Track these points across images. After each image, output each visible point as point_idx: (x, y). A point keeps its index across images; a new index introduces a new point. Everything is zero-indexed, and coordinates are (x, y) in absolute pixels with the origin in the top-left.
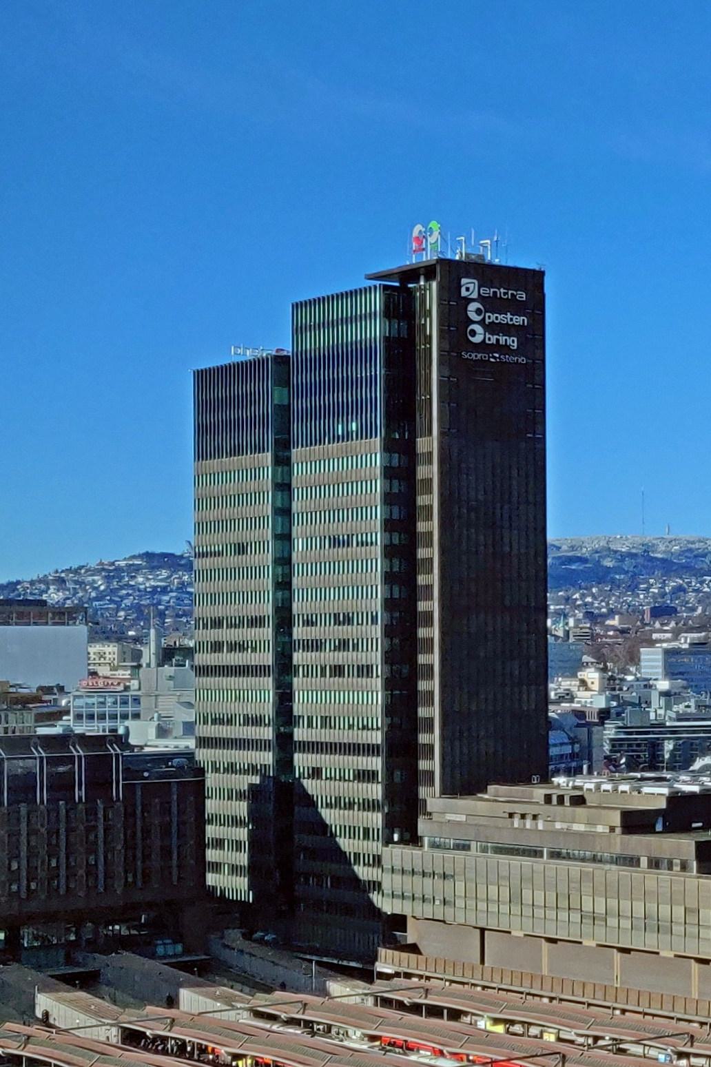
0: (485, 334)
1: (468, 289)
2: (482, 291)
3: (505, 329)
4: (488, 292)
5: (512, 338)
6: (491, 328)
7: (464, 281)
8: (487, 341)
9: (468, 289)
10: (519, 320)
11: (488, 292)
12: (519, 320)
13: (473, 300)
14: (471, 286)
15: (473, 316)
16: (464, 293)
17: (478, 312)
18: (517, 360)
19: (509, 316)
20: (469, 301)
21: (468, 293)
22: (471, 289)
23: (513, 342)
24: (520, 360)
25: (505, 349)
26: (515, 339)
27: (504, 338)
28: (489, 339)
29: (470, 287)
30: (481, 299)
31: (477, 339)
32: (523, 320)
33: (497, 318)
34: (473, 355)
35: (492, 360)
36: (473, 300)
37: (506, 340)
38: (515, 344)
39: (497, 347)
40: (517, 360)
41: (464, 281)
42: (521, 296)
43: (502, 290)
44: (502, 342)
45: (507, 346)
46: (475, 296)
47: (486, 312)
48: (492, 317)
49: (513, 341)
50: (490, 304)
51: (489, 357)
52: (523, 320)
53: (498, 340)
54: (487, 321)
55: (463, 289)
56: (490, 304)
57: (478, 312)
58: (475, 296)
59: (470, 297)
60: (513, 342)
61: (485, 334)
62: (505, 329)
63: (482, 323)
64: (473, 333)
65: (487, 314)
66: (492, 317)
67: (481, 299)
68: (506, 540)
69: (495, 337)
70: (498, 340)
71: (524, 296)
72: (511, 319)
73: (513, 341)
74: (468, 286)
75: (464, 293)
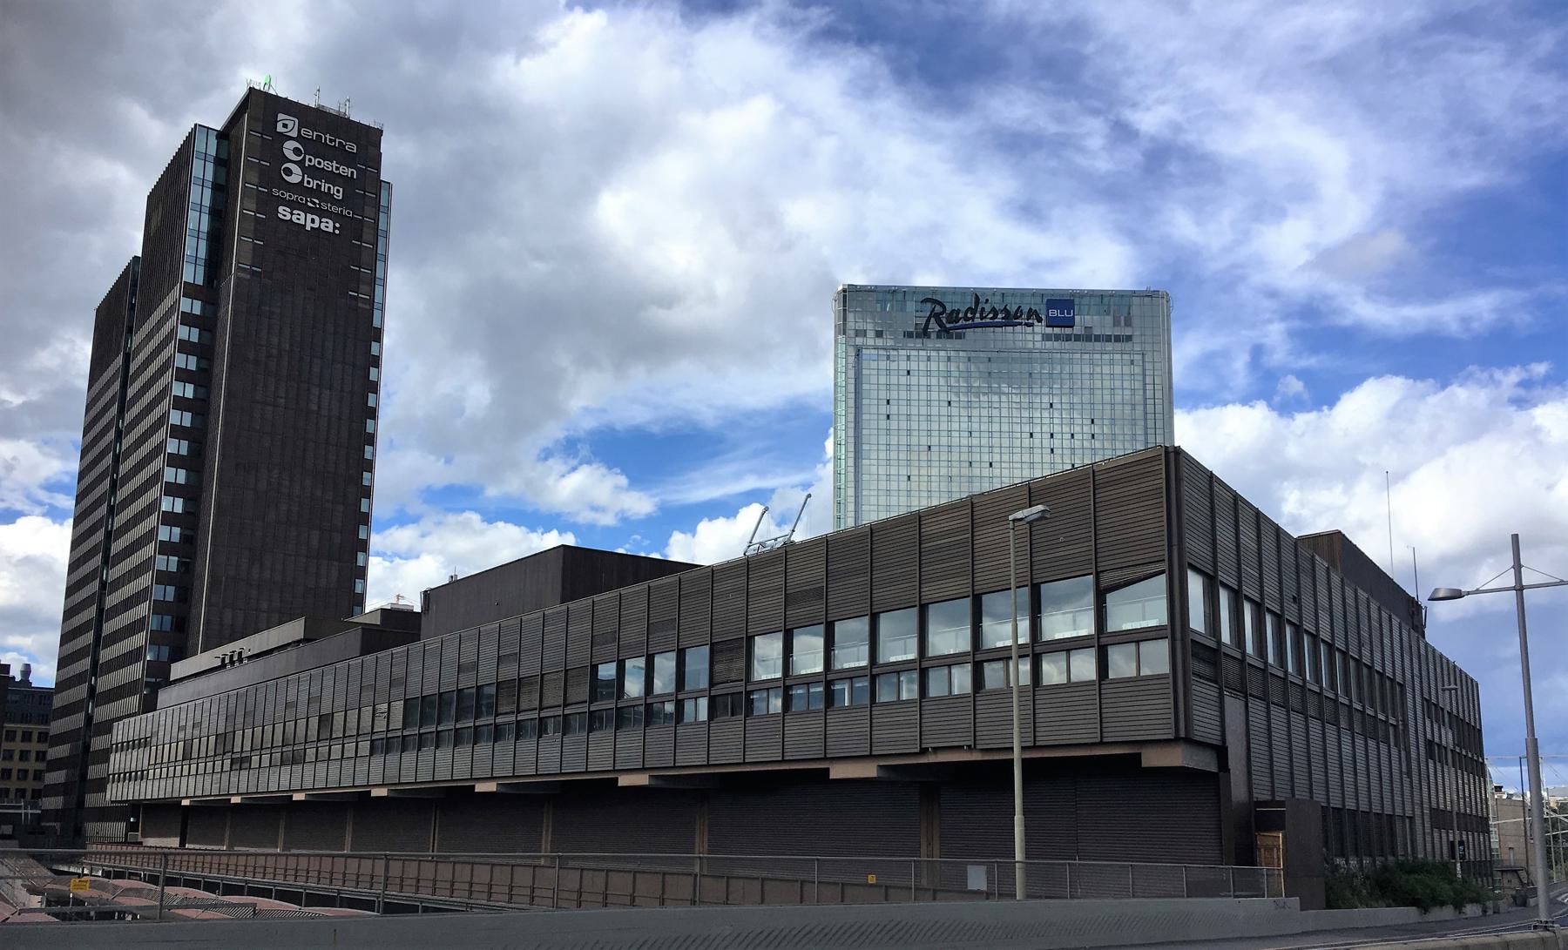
0: (303, 176)
1: (285, 126)
3: (333, 178)
7: (281, 116)
9: (285, 126)
14: (290, 125)
16: (280, 128)
17: (296, 151)
18: (342, 211)
21: (285, 130)
22: (290, 127)
26: (341, 190)
30: (299, 139)
31: (294, 179)
37: (329, 188)
38: (341, 194)
40: (342, 211)
41: (281, 116)
43: (328, 136)
46: (294, 134)
51: (307, 201)
54: (307, 163)
58: (294, 134)
61: (303, 176)
62: (333, 178)
63: (300, 164)
64: (289, 172)
72: (337, 168)
74: (284, 122)
75: (280, 128)
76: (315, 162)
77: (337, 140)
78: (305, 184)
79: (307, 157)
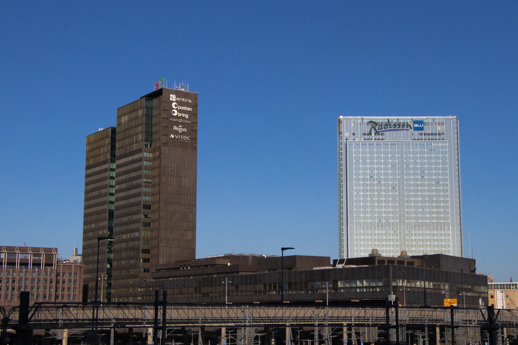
1: (172, 98)
2: (177, 99)
4: (179, 99)
5: (186, 115)
6: (180, 111)
7: (171, 95)
8: (178, 115)
9: (172, 98)
10: (189, 109)
11: (179, 99)
12: (189, 109)
13: (174, 102)
15: (174, 107)
16: (171, 99)
17: (176, 106)
19: (186, 107)
20: (172, 102)
22: (173, 98)
23: (187, 116)
24: (189, 122)
25: (184, 118)
26: (188, 115)
27: (184, 115)
28: (179, 114)
30: (176, 101)
31: (175, 114)
32: (190, 109)
33: (182, 108)
34: (174, 120)
35: (180, 121)
36: (174, 102)
38: (188, 117)
39: (182, 117)
41: (171, 95)
42: (190, 101)
43: (184, 99)
44: (183, 116)
45: (185, 117)
46: (175, 100)
47: (178, 106)
48: (180, 108)
49: (187, 116)
50: (179, 103)
52: (190, 109)
53: (182, 115)
54: (178, 109)
55: (171, 98)
56: (179, 103)
57: (176, 106)
58: (175, 100)
59: (173, 101)
60: (187, 116)
63: (177, 109)
64: (174, 112)
65: (178, 107)
66: (180, 108)
67: (176, 101)
69: (181, 114)
70: (182, 115)
71: (191, 101)
72: (186, 109)
73: (187, 116)
74: (172, 97)
75: (171, 99)
76: (180, 108)
77: (186, 100)
78: (178, 115)
79: (178, 107)
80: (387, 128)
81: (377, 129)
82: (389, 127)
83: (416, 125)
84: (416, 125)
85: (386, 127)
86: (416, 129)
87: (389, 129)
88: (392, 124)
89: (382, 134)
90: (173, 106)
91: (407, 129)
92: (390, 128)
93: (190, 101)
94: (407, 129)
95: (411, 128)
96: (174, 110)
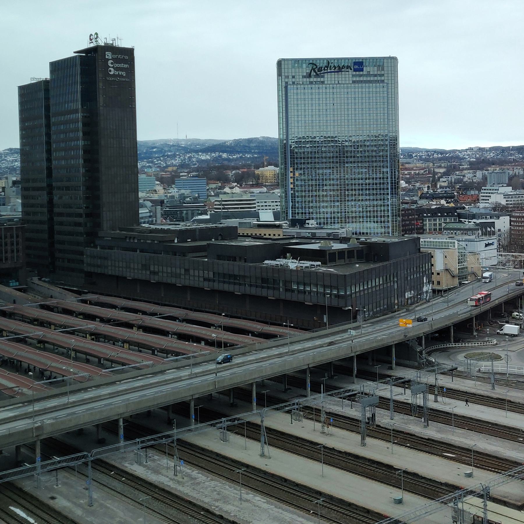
1: (108, 56)
3: (122, 69)
6: (116, 69)
7: (107, 53)
9: (108, 56)
10: (126, 66)
12: (126, 66)
14: (109, 55)
15: (110, 65)
16: (107, 57)
17: (112, 64)
19: (122, 65)
20: (108, 60)
23: (124, 74)
25: (122, 76)
29: (109, 55)
30: (112, 59)
39: (119, 75)
41: (107, 53)
44: (120, 74)
46: (110, 58)
48: (117, 65)
55: (106, 56)
56: (116, 60)
58: (110, 58)
60: (124, 74)
62: (122, 69)
64: (110, 71)
66: (117, 65)
67: (112, 59)
68: (123, 142)
75: (107, 57)
76: (117, 65)
80: (327, 70)
81: (317, 71)
82: (329, 68)
83: (356, 67)
84: (356, 67)
85: (326, 69)
86: (355, 70)
87: (329, 71)
88: (332, 65)
89: (323, 77)
90: (109, 64)
91: (348, 70)
92: (330, 69)
93: (127, 57)
94: (348, 70)
95: (351, 69)
96: (110, 69)
